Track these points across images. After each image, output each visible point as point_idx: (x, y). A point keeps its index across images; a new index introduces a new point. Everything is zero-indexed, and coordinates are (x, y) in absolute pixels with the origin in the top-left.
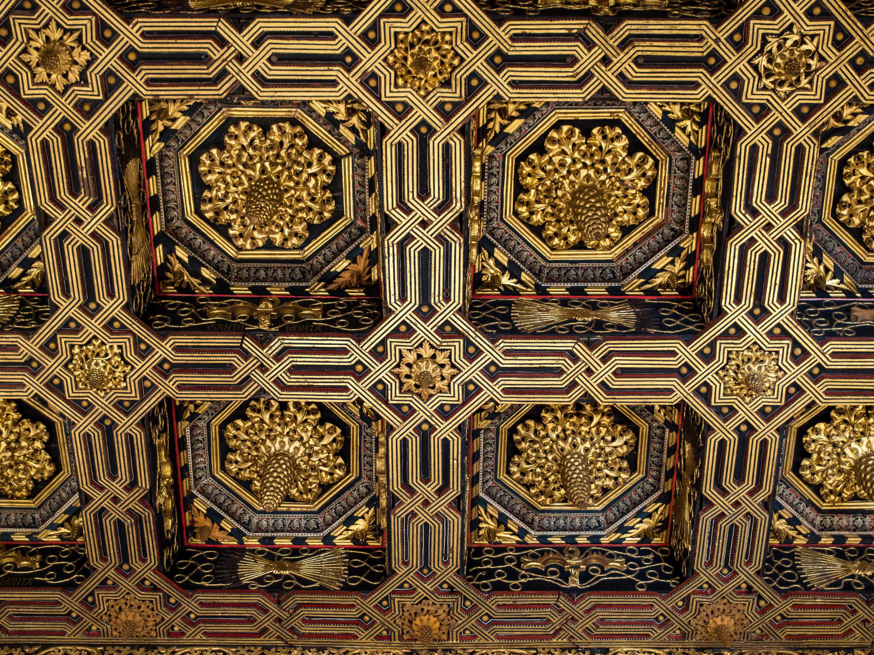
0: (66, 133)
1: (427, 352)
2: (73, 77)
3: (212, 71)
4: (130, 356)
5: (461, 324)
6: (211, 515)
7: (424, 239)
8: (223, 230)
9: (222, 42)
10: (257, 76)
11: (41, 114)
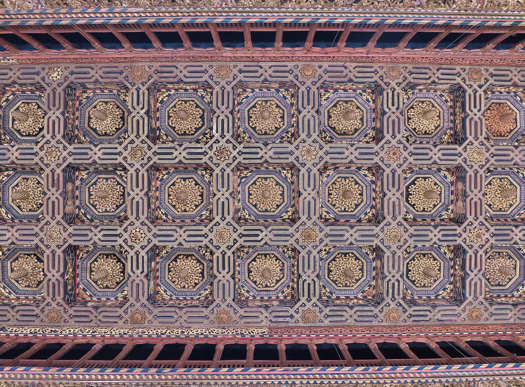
0: (53, 171)
1: (138, 230)
2: (56, 158)
3: (88, 157)
4: (62, 232)
5: (147, 222)
6: (84, 290)
7: (137, 199)
8: (95, 206)
9: (92, 150)
10: (99, 157)
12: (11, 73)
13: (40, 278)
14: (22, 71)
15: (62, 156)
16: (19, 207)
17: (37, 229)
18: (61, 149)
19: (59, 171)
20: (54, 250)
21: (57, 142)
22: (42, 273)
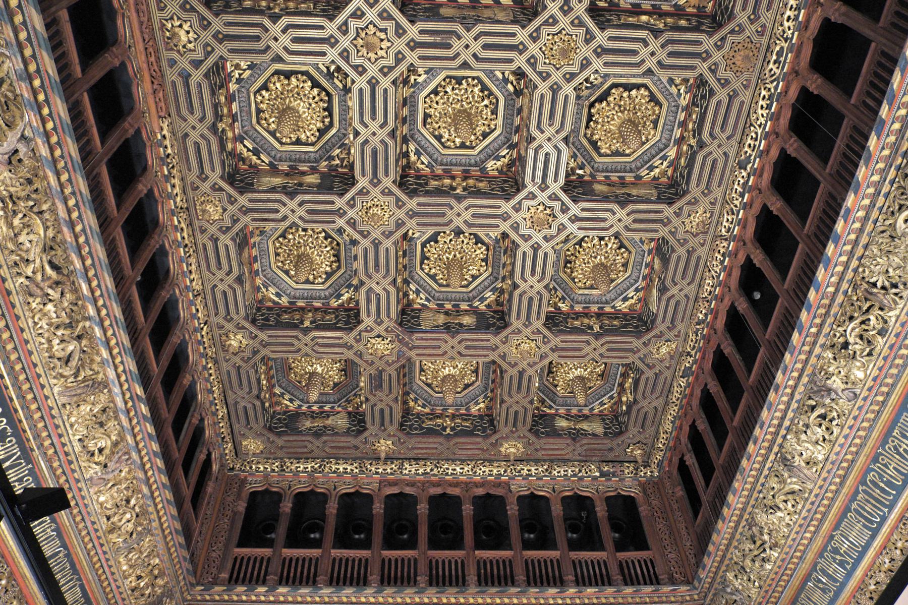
11: (404, 57)
12: (194, 136)
13: (643, 97)
14: (184, 112)
15: (378, 21)
16: (485, 135)
17: (543, 87)
18: (361, 24)
19: (413, 31)
20: (595, 51)
21: (345, 33)
22: (634, 92)
